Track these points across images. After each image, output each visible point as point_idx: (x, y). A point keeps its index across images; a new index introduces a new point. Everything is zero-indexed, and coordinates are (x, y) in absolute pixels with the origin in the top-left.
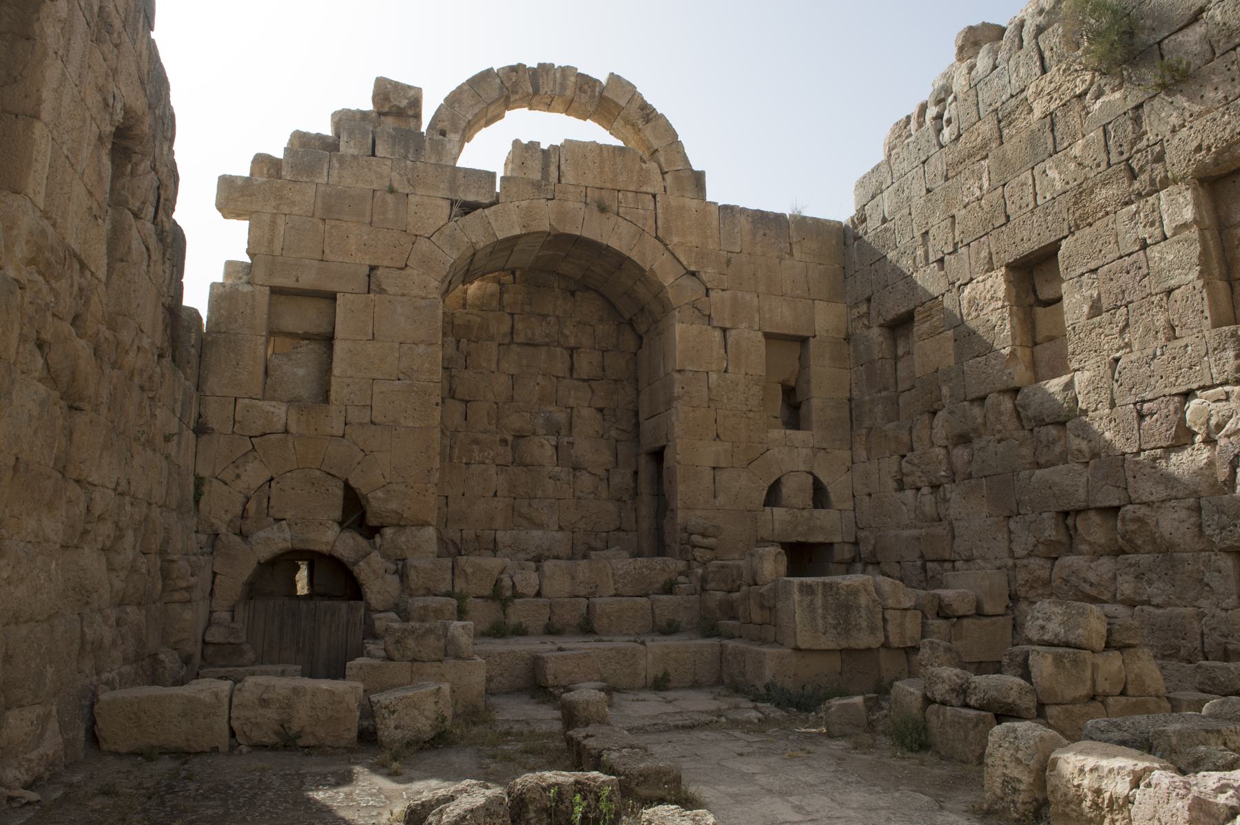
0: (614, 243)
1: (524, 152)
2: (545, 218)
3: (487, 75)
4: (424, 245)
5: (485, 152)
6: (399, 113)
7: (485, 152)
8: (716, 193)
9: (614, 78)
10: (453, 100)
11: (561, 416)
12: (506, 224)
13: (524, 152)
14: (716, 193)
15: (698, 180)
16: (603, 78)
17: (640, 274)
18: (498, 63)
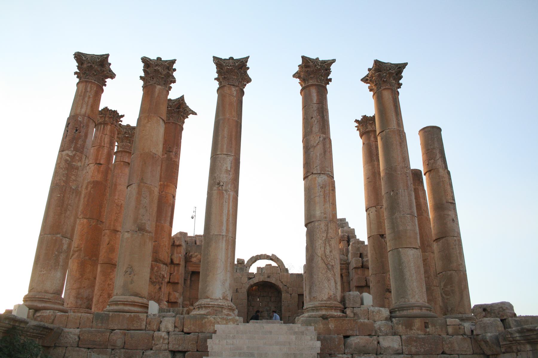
0: (273, 282)
1: (259, 269)
2: (262, 279)
3: (253, 257)
4: (244, 285)
5: (253, 269)
6: (241, 264)
7: (253, 269)
8: (290, 272)
9: (273, 255)
10: (248, 262)
11: (268, 308)
12: (256, 280)
13: (259, 269)
14: (290, 272)
15: (287, 270)
16: (271, 255)
17: (278, 286)
18: (255, 255)
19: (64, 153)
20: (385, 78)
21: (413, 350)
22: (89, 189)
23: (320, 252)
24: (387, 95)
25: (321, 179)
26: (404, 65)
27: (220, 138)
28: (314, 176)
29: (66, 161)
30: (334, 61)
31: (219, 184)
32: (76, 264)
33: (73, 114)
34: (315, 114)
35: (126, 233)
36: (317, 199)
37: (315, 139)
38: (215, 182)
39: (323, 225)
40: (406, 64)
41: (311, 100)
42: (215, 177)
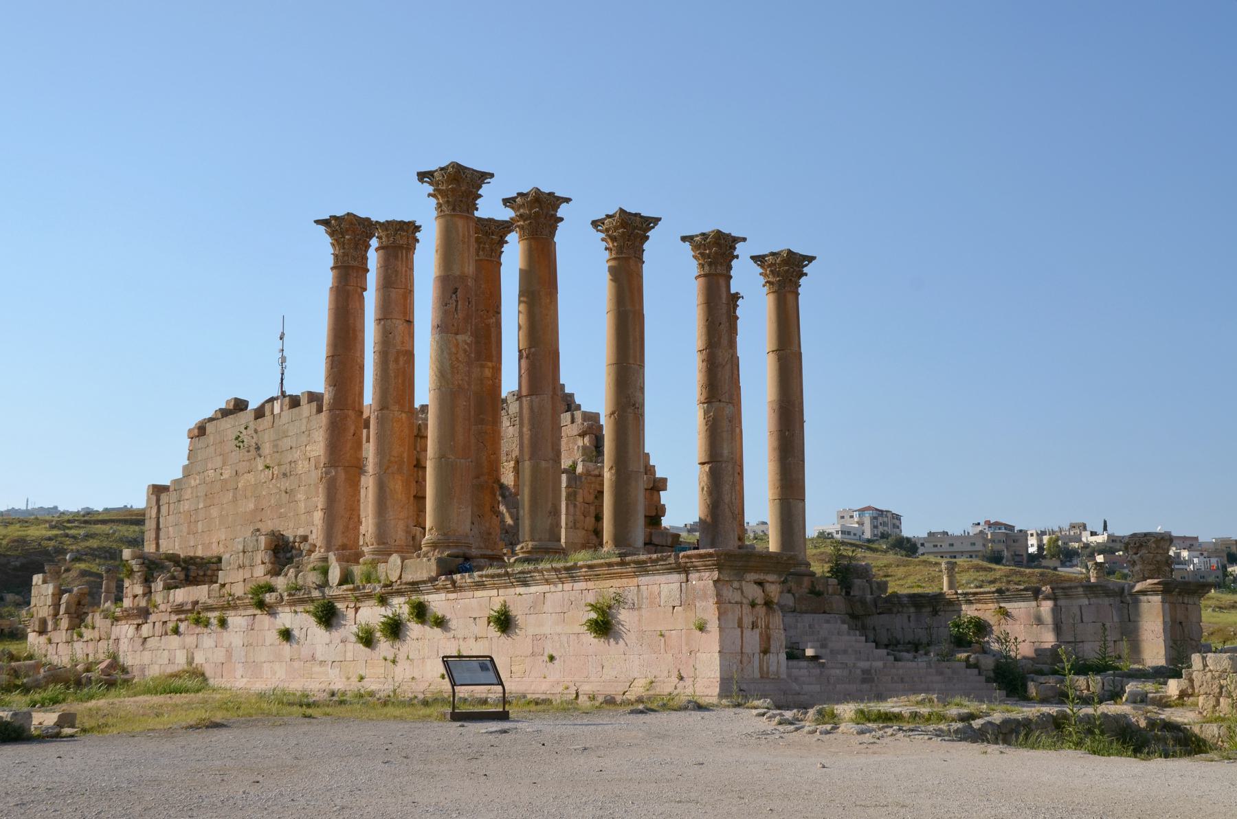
19: (460, 338)
20: (786, 271)
21: (804, 608)
22: (401, 362)
23: (727, 499)
24: (790, 297)
25: (728, 410)
26: (811, 259)
28: (722, 405)
29: (465, 351)
30: (744, 239)
32: (400, 483)
33: (458, 273)
34: (724, 319)
36: (725, 435)
37: (722, 356)
39: (730, 468)
40: (811, 259)
41: (720, 298)
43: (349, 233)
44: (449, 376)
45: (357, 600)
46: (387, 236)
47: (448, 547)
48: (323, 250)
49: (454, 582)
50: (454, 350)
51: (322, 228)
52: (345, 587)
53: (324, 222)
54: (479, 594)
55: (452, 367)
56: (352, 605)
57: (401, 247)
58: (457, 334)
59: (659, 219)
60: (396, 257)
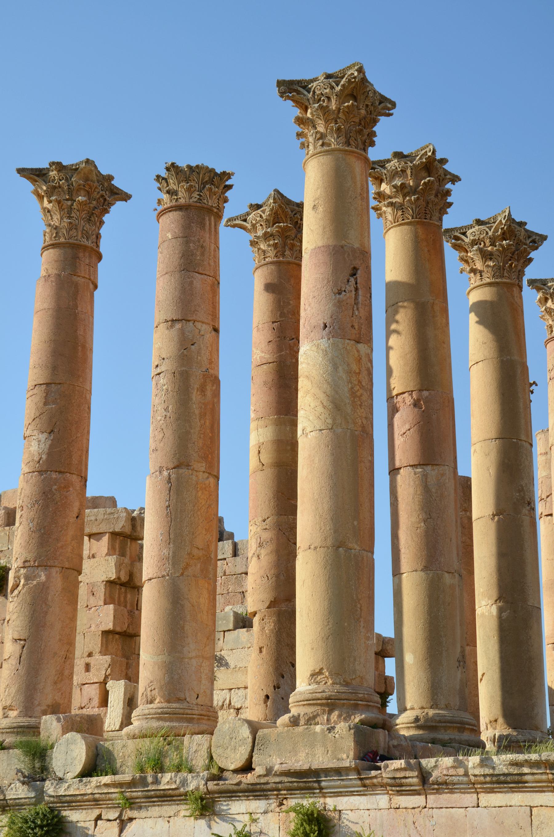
27: (521, 405)
31: (529, 503)
35: (446, 575)
38: (523, 498)
42: (522, 486)
43: (80, 198)
44: (349, 409)
45: (131, 803)
46: (189, 190)
47: (356, 707)
48: (31, 219)
49: (424, 776)
50: (355, 367)
51: (27, 185)
52: (94, 780)
53: (35, 175)
54: (486, 799)
55: (353, 394)
56: (113, 814)
57: (209, 210)
58: (358, 342)
59: (544, 238)
60: (202, 225)
